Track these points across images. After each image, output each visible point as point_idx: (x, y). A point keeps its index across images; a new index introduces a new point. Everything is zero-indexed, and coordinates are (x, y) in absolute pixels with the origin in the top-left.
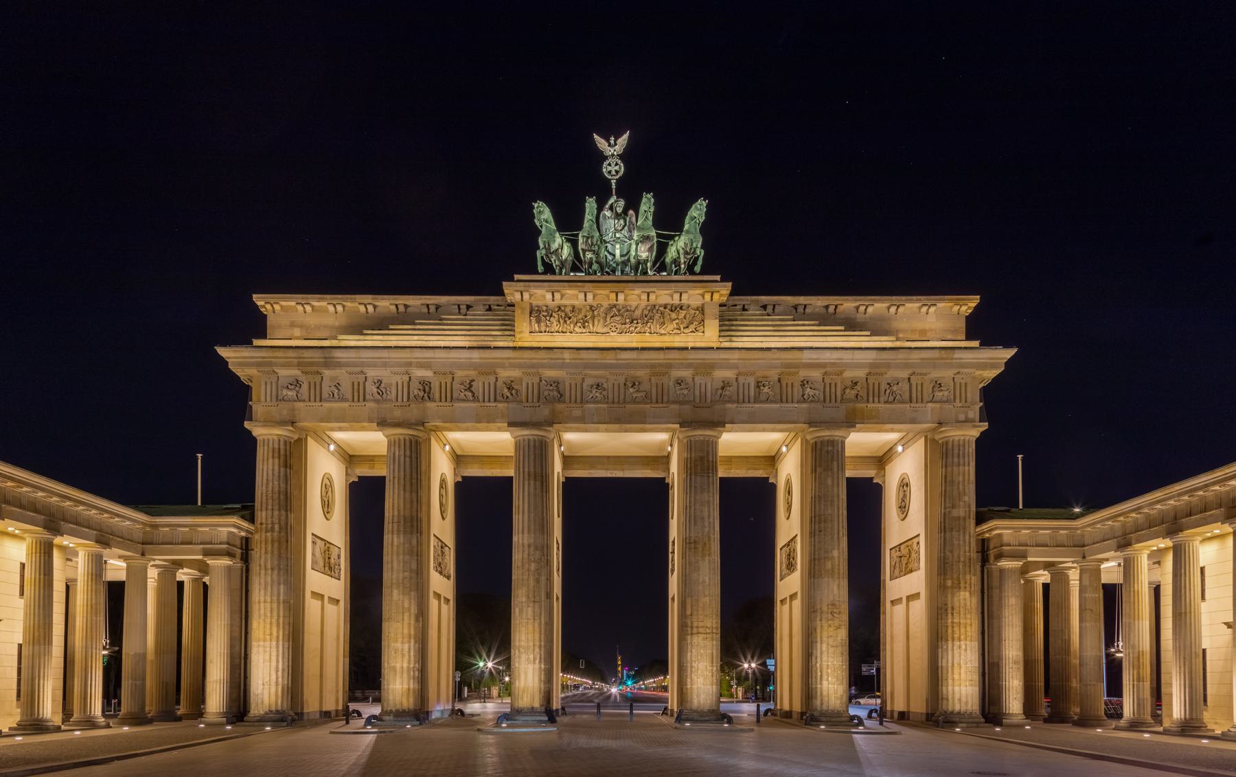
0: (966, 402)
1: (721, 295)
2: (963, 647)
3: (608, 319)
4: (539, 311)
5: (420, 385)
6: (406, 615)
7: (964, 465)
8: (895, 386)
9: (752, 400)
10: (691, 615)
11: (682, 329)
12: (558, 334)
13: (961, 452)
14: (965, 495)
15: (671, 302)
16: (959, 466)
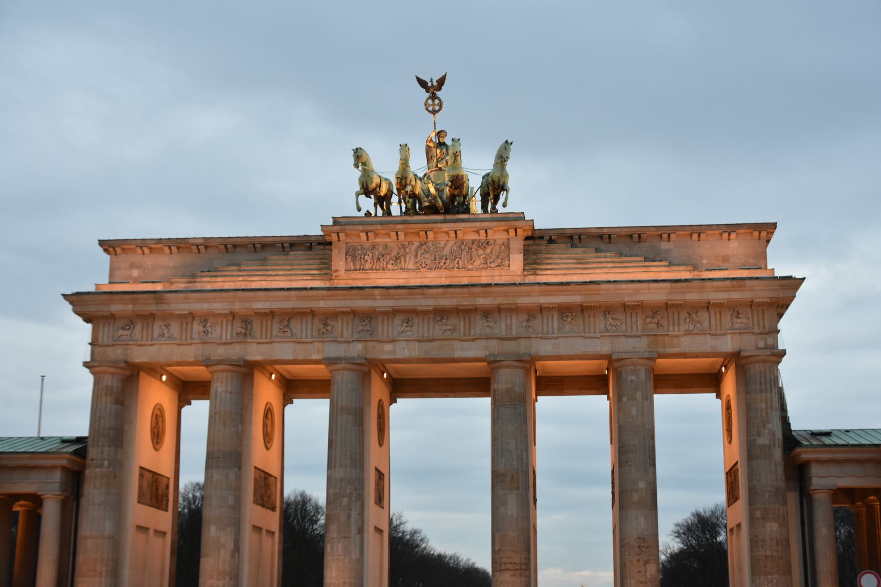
0: (764, 328)
1: (524, 230)
2: (775, 581)
3: (419, 256)
4: (355, 249)
5: (243, 324)
6: (222, 551)
7: (766, 392)
8: (694, 315)
9: (555, 332)
10: (500, 550)
11: (488, 263)
12: (371, 271)
13: (763, 379)
14: (768, 423)
15: (479, 238)
16: (761, 392)
